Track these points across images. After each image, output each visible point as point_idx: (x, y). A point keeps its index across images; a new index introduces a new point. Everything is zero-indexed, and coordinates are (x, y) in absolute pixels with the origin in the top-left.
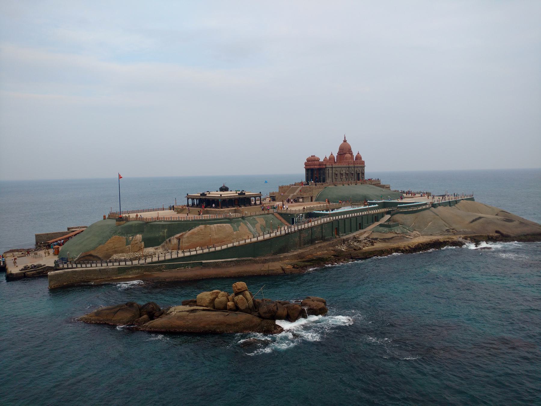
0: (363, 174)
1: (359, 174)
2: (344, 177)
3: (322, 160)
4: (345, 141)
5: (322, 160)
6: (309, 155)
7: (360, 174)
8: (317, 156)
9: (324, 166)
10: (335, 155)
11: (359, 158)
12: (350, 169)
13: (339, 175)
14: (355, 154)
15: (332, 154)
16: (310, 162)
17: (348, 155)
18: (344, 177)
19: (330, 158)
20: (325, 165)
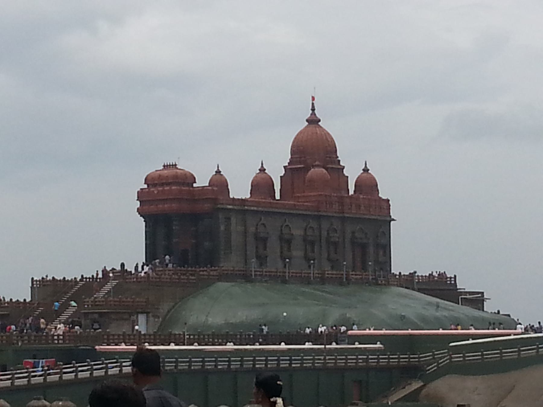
0: (385, 248)
1: (364, 247)
2: (297, 253)
3: (202, 181)
4: (313, 121)
5: (202, 181)
6: (155, 166)
7: (371, 250)
8: (185, 166)
9: (207, 206)
10: (276, 173)
11: (367, 184)
12: (325, 225)
13: (274, 244)
14: (352, 173)
15: (262, 170)
16: (154, 190)
17: (317, 172)
18: (297, 253)
19: (255, 187)
20: (215, 201)
